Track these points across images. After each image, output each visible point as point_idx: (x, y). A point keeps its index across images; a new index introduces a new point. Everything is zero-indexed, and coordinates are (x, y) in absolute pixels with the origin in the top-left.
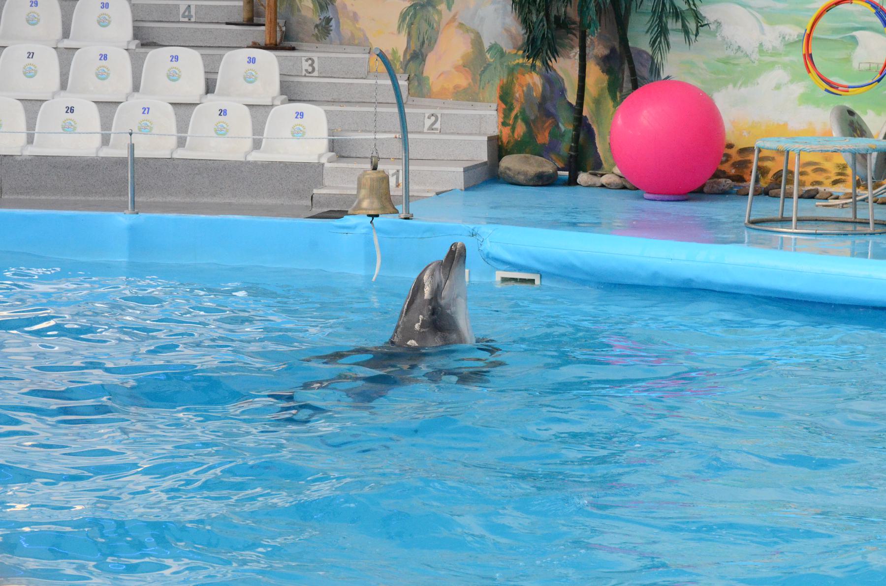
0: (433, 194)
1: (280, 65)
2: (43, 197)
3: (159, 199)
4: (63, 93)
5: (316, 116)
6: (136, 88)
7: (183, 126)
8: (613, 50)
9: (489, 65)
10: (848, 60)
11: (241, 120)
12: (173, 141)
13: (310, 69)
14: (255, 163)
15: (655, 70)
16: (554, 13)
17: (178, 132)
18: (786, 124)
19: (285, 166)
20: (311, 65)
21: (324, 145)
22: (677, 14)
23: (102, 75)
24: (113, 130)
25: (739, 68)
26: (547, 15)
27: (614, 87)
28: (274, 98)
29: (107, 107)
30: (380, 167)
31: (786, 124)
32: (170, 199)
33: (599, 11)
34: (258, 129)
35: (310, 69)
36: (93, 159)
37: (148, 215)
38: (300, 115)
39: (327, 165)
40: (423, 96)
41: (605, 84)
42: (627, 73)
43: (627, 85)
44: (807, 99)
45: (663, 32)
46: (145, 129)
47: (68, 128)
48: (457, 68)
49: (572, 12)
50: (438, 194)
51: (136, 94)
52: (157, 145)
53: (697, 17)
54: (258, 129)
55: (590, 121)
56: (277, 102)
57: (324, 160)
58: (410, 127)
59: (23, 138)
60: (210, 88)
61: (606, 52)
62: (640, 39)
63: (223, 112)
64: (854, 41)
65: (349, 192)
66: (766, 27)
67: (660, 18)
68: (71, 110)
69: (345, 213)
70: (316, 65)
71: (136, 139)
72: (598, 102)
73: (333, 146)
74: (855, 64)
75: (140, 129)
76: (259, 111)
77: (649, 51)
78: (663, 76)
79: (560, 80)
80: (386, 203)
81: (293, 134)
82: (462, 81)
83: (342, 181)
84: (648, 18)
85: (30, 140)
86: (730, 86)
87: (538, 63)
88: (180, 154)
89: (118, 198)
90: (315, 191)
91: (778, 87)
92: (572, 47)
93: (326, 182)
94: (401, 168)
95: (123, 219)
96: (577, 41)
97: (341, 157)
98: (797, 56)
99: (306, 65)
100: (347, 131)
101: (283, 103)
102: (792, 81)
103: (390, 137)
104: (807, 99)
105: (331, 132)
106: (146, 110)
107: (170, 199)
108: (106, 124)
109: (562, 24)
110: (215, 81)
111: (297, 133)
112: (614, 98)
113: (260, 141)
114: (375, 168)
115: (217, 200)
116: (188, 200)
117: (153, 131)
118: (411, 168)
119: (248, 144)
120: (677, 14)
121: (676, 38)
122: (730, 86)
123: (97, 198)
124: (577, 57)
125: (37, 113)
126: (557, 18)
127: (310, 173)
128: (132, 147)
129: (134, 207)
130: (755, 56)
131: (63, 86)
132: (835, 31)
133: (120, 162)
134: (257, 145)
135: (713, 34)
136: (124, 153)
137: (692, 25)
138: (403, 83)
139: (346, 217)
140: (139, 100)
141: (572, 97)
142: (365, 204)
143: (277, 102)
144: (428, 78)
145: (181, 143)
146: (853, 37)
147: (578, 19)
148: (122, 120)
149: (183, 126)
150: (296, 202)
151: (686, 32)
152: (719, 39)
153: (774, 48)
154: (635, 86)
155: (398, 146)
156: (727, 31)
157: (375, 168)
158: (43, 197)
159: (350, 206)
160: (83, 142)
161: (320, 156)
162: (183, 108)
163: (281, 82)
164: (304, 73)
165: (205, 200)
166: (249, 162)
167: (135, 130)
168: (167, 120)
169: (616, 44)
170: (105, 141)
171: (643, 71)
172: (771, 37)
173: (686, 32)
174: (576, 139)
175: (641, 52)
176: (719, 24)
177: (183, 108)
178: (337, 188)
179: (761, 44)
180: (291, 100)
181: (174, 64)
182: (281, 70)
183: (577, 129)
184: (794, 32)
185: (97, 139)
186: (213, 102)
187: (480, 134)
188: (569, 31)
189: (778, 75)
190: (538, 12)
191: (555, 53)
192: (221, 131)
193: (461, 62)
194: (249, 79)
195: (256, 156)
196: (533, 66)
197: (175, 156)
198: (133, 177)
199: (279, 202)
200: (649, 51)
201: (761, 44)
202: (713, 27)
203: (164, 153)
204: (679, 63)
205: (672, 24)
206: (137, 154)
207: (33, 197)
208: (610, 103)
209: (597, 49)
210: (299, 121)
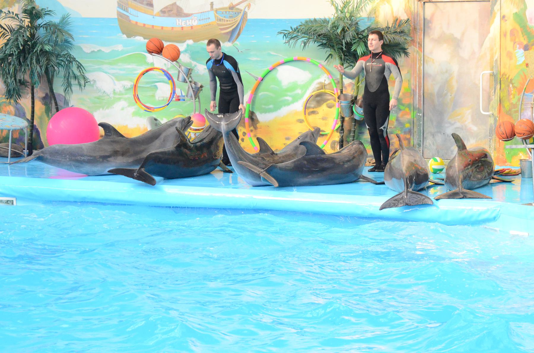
8: (47, 94)
10: (154, 96)
15: (66, 103)
16: (18, 78)
18: (127, 126)
22: (75, 77)
25: (104, 100)
26: (15, 79)
27: (48, 111)
31: (127, 126)
33: (39, 77)
41: (44, 110)
42: (54, 104)
43: (54, 110)
44: (135, 114)
45: (69, 85)
49: (27, 77)
53: (84, 78)
55: (37, 127)
61: (44, 95)
62: (59, 88)
64: (156, 87)
66: (116, 81)
67: (68, 79)
72: (41, 118)
74: (157, 98)
77: (63, 94)
78: (70, 105)
79: (23, 109)
84: (62, 79)
86: (101, 109)
87: (12, 101)
91: (123, 109)
92: (28, 94)
96: (30, 91)
98: (131, 95)
102: (129, 106)
104: (135, 114)
109: (22, 83)
112: (48, 116)
120: (75, 77)
121: (75, 88)
122: (101, 109)
124: (30, 98)
126: (20, 80)
130: (112, 95)
132: (147, 83)
135: (92, 86)
137: (82, 82)
141: (29, 116)
146: (155, 86)
147: (29, 80)
151: (80, 85)
152: (95, 88)
153: (120, 91)
154: (57, 110)
156: (99, 84)
169: (48, 91)
171: (60, 103)
172: (119, 86)
173: (80, 85)
174: (32, 134)
175: (60, 95)
176: (95, 81)
179: (114, 90)
183: (31, 131)
184: (129, 84)
188: (26, 86)
189: (122, 103)
190: (11, 78)
191: (20, 96)
196: (10, 103)
200: (63, 94)
201: (114, 90)
202: (92, 83)
204: (77, 99)
205: (73, 82)
208: (46, 118)
209: (39, 93)
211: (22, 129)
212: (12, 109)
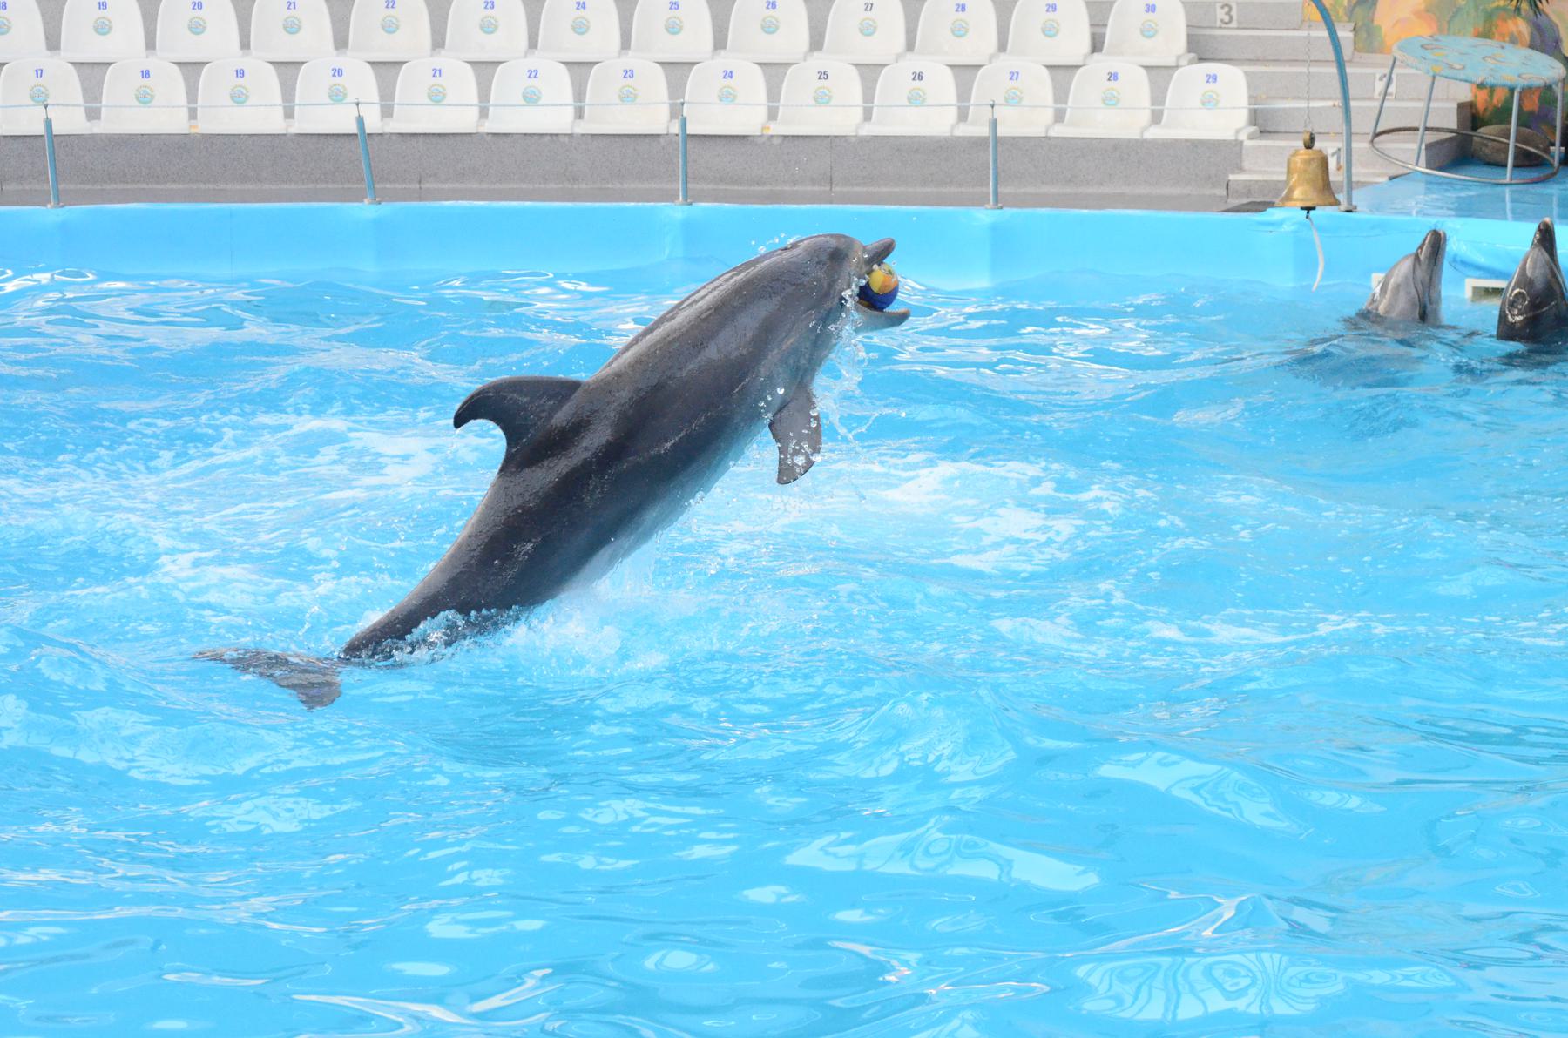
0: (1384, 179)
1: (1188, 14)
2: (884, 189)
3: (1030, 190)
4: (909, 55)
5: (1233, 81)
6: (1002, 47)
7: (1061, 94)
9: (1460, 9)
11: (1137, 87)
12: (1049, 115)
13: (1227, 19)
14: (1154, 143)
17: (1056, 100)
19: (1195, 145)
20: (1228, 13)
21: (1242, 117)
23: (959, 31)
24: (973, 101)
28: (1179, 57)
29: (965, 73)
30: (1317, 145)
32: (1045, 189)
34: (1158, 96)
35: (1227, 19)
36: (946, 139)
37: (1015, 210)
38: (1213, 78)
39: (1248, 143)
40: (1374, 52)
46: (1013, 99)
47: (916, 100)
48: (1417, 14)
50: (1391, 178)
51: (1002, 56)
52: (1028, 118)
54: (1158, 96)
56: (1183, 62)
57: (1243, 137)
58: (1352, 92)
59: (858, 114)
60: (1097, 45)
63: (1113, 76)
65: (1275, 178)
68: (919, 76)
69: (1271, 205)
70: (1234, 13)
71: (999, 112)
73: (1255, 117)
75: (1006, 100)
76: (1159, 75)
79: (1554, 27)
80: (1326, 190)
81: (1203, 103)
82: (1423, 30)
83: (1269, 163)
85: (867, 116)
88: (1058, 131)
89: (978, 189)
90: (1231, 177)
93: (1246, 165)
94: (1341, 144)
95: (984, 216)
97: (1264, 132)
99: (1221, 14)
100: (1274, 98)
101: (1191, 62)
103: (1328, 104)
105: (1252, 98)
106: (1014, 75)
107: (1045, 189)
108: (964, 93)
110: (1103, 36)
111: (1208, 102)
113: (1161, 112)
114: (1309, 145)
115: (1106, 189)
116: (1068, 190)
117: (1024, 103)
118: (1354, 145)
119: (1145, 116)
123: (954, 189)
125: (876, 81)
127: (1226, 153)
128: (994, 124)
129: (996, 202)
131: (910, 46)
133: (978, 143)
134: (1156, 118)
136: (983, 131)
138: (1345, 34)
139: (1270, 210)
140: (1006, 62)
142: (1297, 194)
143: (1183, 62)
144: (1379, 28)
145: (1059, 116)
148: (983, 88)
149: (1061, 94)
150: (1208, 191)
155: (1339, 115)
157: (1309, 145)
158: (884, 189)
159: (1277, 195)
160: (934, 118)
161: (1238, 131)
162: (1062, 72)
163: (1189, 36)
164: (1219, 23)
165: (1090, 190)
166: (1145, 141)
167: (999, 100)
168: (1041, 87)
170: (963, 116)
177: (1062, 72)
178: (1260, 172)
180: (1201, 60)
181: (1051, 15)
182: (1188, 19)
185: (952, 114)
186: (1101, 64)
187: (1447, 100)
192: (1110, 101)
193: (1423, 7)
194: (1148, 32)
195: (1155, 133)
196: (1518, 9)
197: (1052, 134)
198: (995, 161)
199: (1186, 191)
203: (1036, 131)
206: (1001, 132)
207: (871, 189)
210: (1211, 86)
211: (1548, 88)
212: (1522, 27)
